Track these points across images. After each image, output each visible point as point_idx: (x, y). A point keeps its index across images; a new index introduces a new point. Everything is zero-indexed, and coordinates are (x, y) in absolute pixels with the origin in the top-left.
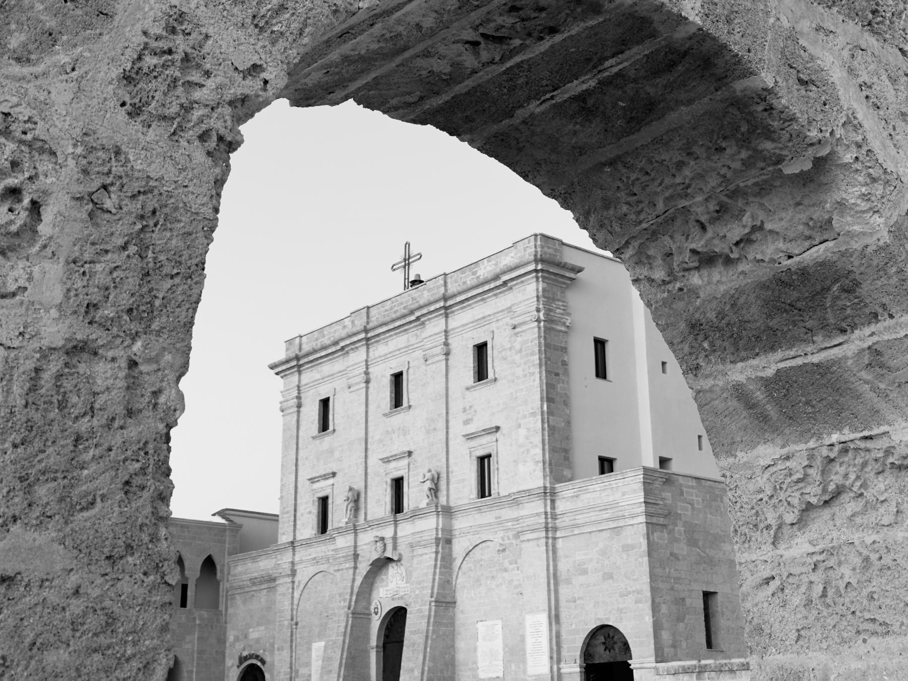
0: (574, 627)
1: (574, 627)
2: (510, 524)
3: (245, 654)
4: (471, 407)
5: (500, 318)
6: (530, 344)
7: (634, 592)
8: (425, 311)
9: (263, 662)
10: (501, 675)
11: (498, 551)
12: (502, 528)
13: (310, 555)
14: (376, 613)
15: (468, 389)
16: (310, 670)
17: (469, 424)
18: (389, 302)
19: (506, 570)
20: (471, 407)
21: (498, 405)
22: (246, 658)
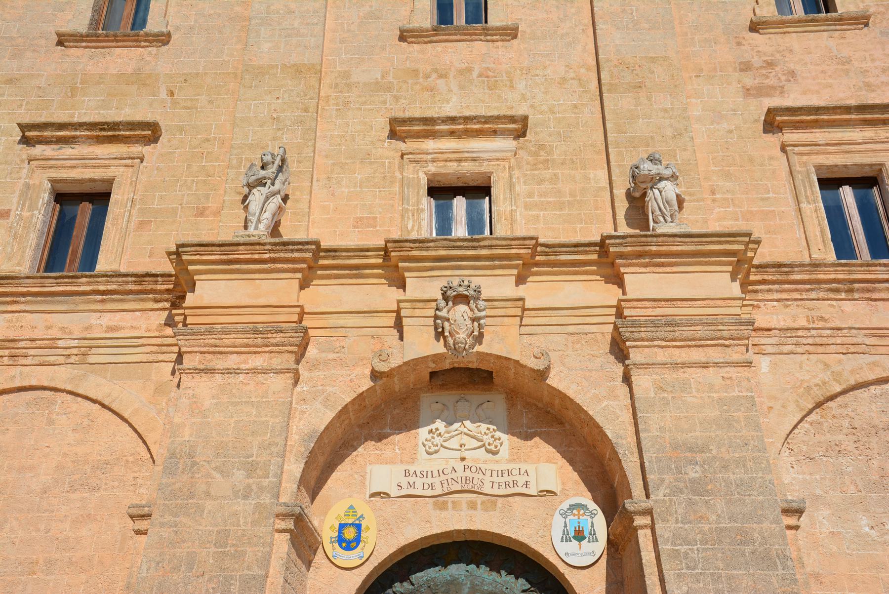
4: (770, 64)
14: (348, 545)
15: (755, 27)
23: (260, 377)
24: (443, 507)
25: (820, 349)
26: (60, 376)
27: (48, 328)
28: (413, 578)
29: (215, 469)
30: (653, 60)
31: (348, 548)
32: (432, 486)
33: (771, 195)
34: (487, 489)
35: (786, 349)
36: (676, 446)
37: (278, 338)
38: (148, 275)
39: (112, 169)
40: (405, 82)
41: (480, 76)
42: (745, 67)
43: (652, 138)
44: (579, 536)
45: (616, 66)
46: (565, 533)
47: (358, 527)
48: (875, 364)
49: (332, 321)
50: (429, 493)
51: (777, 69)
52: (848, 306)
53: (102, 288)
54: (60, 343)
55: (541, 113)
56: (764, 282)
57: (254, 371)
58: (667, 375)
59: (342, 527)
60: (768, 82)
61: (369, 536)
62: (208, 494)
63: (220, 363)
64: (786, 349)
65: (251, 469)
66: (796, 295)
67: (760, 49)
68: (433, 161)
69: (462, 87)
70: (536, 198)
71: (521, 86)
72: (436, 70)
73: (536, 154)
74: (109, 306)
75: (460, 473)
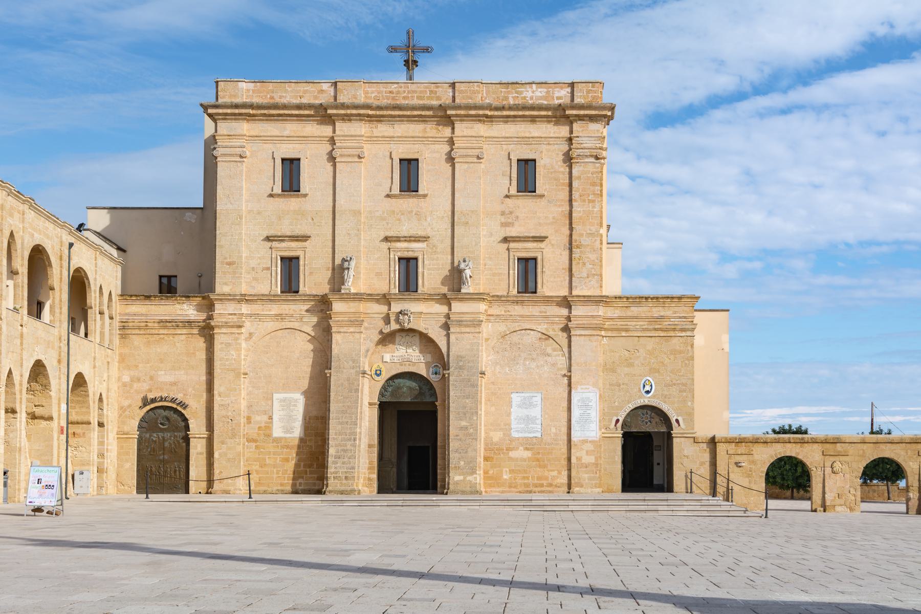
0: (616, 404)
1: (616, 404)
2: (557, 319)
3: (151, 396)
4: (511, 213)
5: (551, 143)
6: (590, 175)
7: (678, 384)
8: (462, 112)
9: (185, 406)
10: (539, 435)
11: (540, 339)
12: (546, 322)
13: (270, 310)
14: (378, 375)
16: (271, 418)
17: (509, 226)
18: (396, 85)
19: (549, 355)
20: (511, 213)
21: (546, 217)
22: (153, 400)
23: (353, 334)
24: (402, 365)
25: (506, 321)
26: (296, 325)
27: (290, 310)
28: (395, 380)
29: (345, 361)
30: (472, 211)
31: (378, 376)
32: (399, 360)
33: (502, 267)
34: (413, 361)
35: (497, 321)
36: (458, 356)
37: (357, 323)
38: (316, 295)
39: (298, 251)
40: (390, 216)
41: (415, 214)
42: (503, 213)
43: (468, 245)
44: (436, 373)
45: (460, 214)
46: (433, 372)
47: (380, 371)
48: (520, 325)
49: (372, 315)
50: (398, 362)
51: (513, 215)
52: (516, 307)
53: (303, 298)
54: (294, 316)
55: (435, 231)
56: (493, 300)
57: (351, 332)
58: (459, 335)
59: (376, 370)
60: (510, 220)
61: (383, 373)
62: (344, 368)
63: (342, 330)
64: (497, 321)
66: (503, 304)
67: (509, 206)
68: (400, 251)
69: (409, 220)
70: (431, 266)
71: (429, 219)
72: (400, 211)
73: (432, 249)
74: (305, 303)
75: (406, 356)
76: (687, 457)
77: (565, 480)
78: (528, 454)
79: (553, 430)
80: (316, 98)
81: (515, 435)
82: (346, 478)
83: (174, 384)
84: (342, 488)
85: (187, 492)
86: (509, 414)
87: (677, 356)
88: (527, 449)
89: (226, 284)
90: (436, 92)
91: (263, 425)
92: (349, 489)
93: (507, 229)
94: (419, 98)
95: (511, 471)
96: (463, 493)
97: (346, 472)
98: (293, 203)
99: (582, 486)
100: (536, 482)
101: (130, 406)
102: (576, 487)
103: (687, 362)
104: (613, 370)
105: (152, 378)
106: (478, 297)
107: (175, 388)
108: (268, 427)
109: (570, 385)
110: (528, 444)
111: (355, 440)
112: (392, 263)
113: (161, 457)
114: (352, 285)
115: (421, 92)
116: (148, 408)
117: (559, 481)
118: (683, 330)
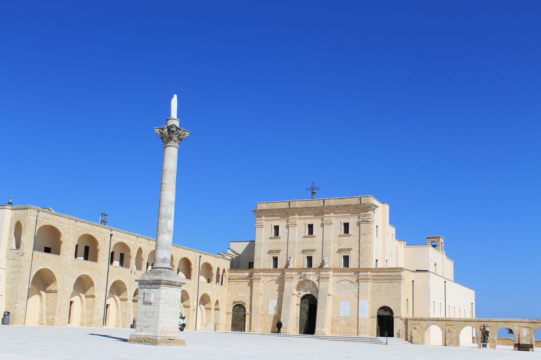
1: (375, 305)
3: (236, 301)
4: (341, 241)
20: (341, 241)
22: (236, 302)
42: (339, 241)
60: (341, 243)
63: (287, 280)
65: (290, 290)
71: (316, 244)
76: (398, 325)
77: (356, 332)
78: (345, 322)
79: (353, 314)
80: (284, 206)
81: (341, 315)
82: (285, 328)
83: (242, 297)
84: (284, 331)
85: (244, 331)
86: (339, 309)
87: (395, 289)
88: (345, 320)
89: (257, 266)
90: (319, 203)
91: (266, 310)
92: (285, 332)
93: (340, 246)
94: (314, 205)
95: (340, 328)
96: (319, 334)
97: (285, 326)
98: (277, 240)
99: (362, 334)
100: (347, 332)
101: (230, 304)
102: (360, 334)
103: (398, 291)
104: (374, 294)
105: (236, 295)
106: (329, 269)
107: (242, 298)
108: (268, 311)
109: (358, 299)
110: (346, 318)
111: (289, 316)
112: (305, 258)
113: (238, 320)
114: (291, 266)
115: (315, 203)
116: (235, 304)
117: (355, 332)
118: (397, 280)
